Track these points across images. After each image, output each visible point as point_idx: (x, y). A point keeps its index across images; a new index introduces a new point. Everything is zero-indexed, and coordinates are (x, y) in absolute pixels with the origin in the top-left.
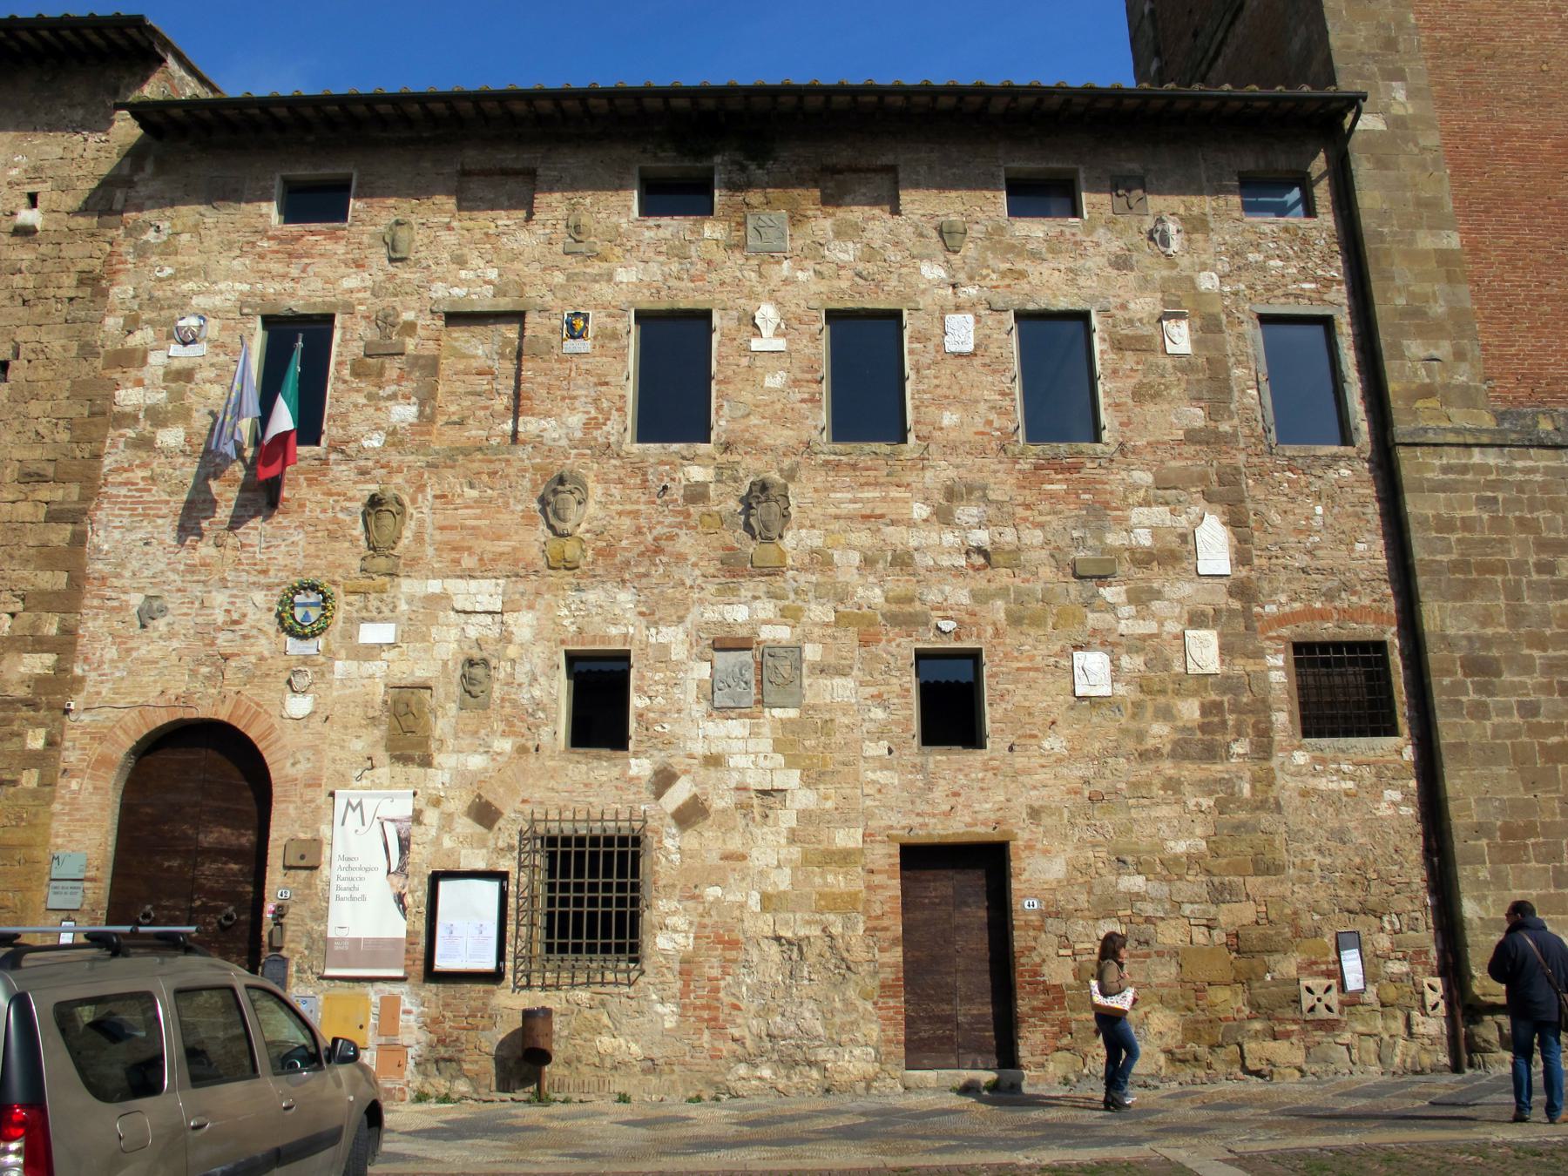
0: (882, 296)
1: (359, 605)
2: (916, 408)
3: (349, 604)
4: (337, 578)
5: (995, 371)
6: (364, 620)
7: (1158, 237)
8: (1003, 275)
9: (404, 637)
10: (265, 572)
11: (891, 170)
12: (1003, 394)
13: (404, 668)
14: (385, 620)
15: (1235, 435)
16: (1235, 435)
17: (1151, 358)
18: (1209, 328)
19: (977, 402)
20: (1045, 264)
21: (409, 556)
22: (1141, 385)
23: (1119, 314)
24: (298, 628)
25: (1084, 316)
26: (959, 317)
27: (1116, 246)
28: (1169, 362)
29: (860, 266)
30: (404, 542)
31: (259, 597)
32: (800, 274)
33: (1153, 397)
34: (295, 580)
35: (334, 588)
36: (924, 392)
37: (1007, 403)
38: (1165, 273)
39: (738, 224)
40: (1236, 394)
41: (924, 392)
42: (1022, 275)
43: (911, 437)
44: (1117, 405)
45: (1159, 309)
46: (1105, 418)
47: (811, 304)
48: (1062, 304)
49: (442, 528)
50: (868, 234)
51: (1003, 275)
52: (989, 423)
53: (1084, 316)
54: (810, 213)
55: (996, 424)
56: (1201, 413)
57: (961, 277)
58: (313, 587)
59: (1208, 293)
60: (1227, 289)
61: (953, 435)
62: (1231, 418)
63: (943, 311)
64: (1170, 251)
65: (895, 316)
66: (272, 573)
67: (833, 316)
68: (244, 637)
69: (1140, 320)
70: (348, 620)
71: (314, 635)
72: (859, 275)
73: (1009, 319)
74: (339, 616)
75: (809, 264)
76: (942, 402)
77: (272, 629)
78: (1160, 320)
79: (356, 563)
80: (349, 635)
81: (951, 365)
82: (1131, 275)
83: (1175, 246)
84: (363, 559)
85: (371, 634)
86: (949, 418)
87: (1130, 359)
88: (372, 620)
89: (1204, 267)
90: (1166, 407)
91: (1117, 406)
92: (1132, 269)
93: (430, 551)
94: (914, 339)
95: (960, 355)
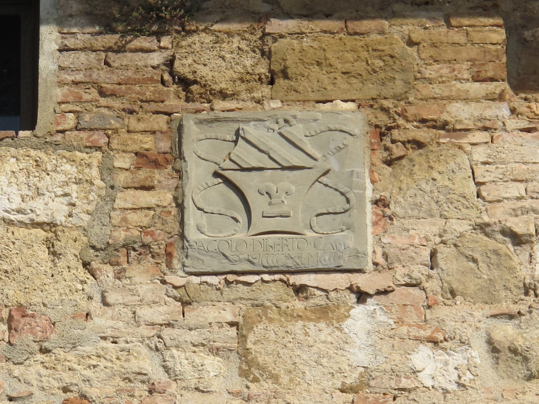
32: (423, 358)
39: (144, 158)
54: (460, 113)
75: (468, 318)
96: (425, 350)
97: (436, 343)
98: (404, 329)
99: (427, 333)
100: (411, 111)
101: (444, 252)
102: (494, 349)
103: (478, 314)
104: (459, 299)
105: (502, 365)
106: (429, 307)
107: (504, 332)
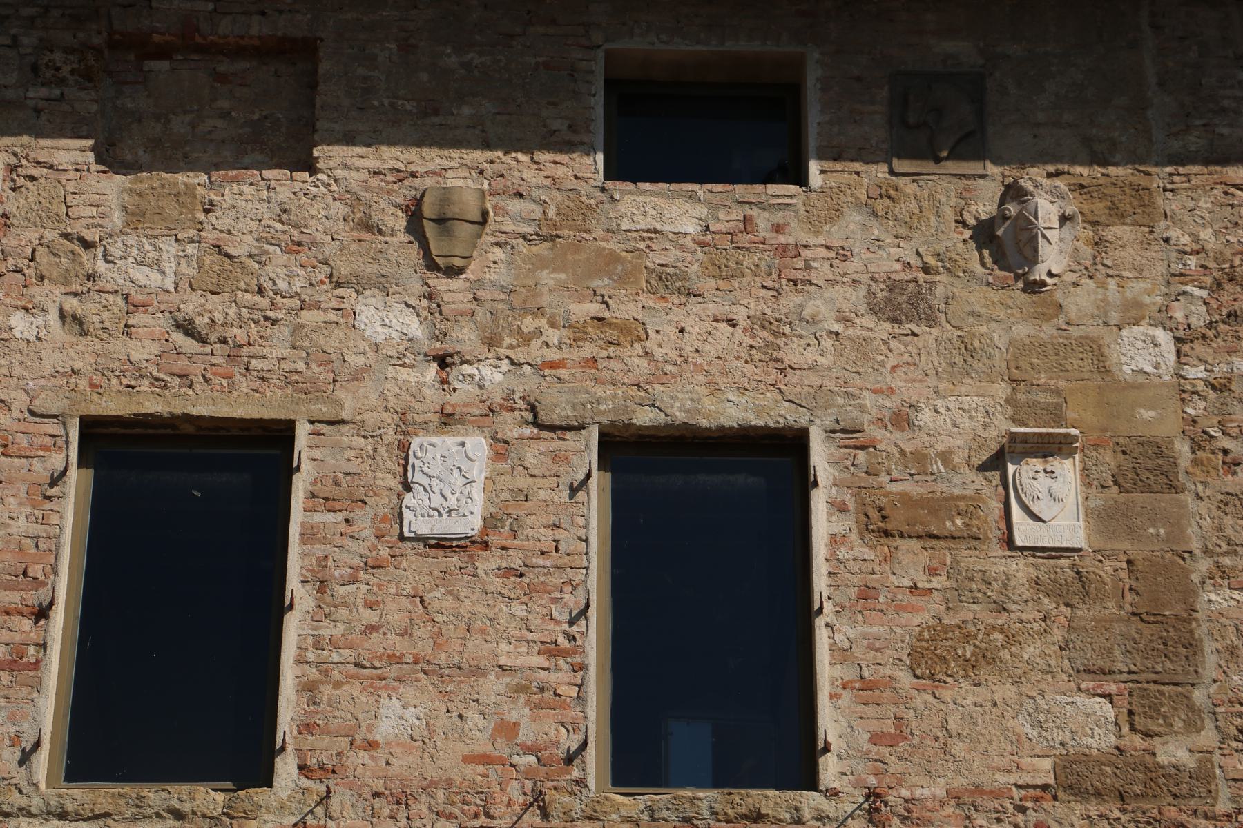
0: (244, 385)
2: (308, 688)
5: (532, 591)
7: (1005, 244)
8: (578, 333)
11: (300, 51)
12: (551, 651)
15: (1203, 775)
16: (1203, 775)
17: (970, 559)
18: (1139, 476)
19: (479, 671)
20: (694, 306)
22: (938, 631)
23: (887, 439)
25: (788, 447)
26: (448, 442)
27: (891, 259)
28: (1020, 569)
29: (191, 305)
33: (970, 665)
36: (335, 644)
37: (561, 678)
38: (1022, 331)
40: (1210, 662)
41: (335, 644)
42: (633, 332)
43: (286, 769)
44: (869, 686)
45: (1003, 426)
46: (830, 721)
47: (45, 403)
48: (732, 410)
50: (221, 219)
51: (578, 333)
52: (508, 730)
53: (788, 447)
55: (526, 735)
56: (1105, 709)
57: (466, 337)
59: (1142, 384)
60: (1196, 373)
61: (404, 763)
62: (1192, 726)
63: (406, 426)
64: (1040, 273)
65: (269, 445)
67: (102, 439)
69: (945, 457)
72: (187, 328)
73: (584, 450)
75: (52, 296)
76: (379, 673)
78: (996, 462)
81: (417, 570)
82: (929, 335)
83: (1054, 256)
86: (395, 716)
87: (912, 560)
89: (1133, 314)
90: (1005, 691)
91: (866, 688)
92: (931, 321)
94: (320, 500)
95: (441, 544)
96: (20, 314)
97: (27, 310)
98: (8, 300)
99: (23, 303)
100: (32, 155)
101: (41, 250)
102: (62, 315)
103: (57, 292)
104: (46, 281)
105: (67, 325)
106: (25, 286)
107: (72, 304)
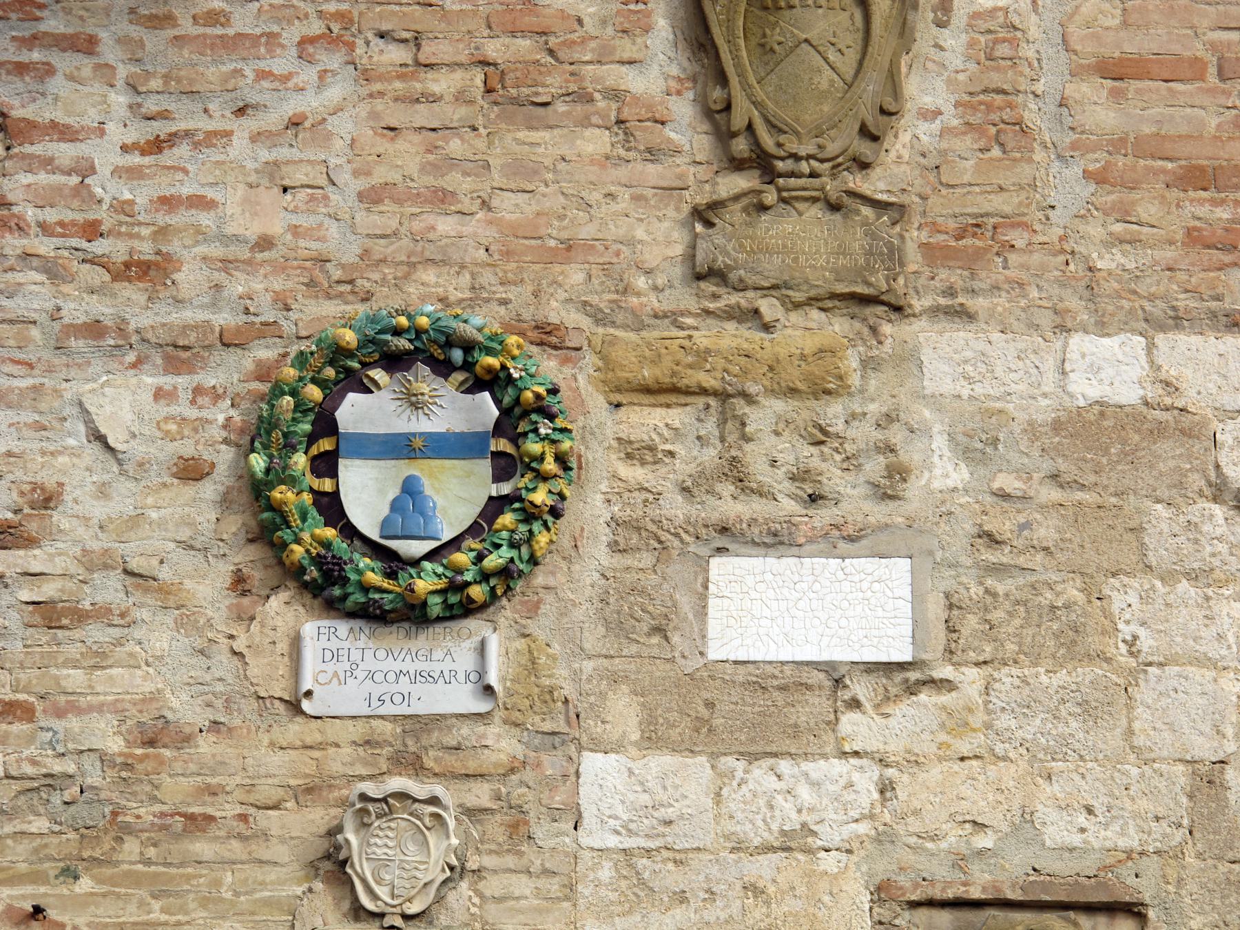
1: (692, 457)
3: (636, 452)
4: (556, 311)
6: (727, 536)
9: (953, 624)
10: (149, 271)
13: (979, 802)
14: (847, 539)
21: (943, 208)
24: (370, 571)
30: (910, 138)
31: (124, 401)
34: (340, 321)
35: (549, 367)
49: (1116, 71)
58: (443, 353)
66: (189, 277)
68: (49, 615)
70: (634, 532)
71: (460, 606)
74: (591, 508)
77: (208, 588)
79: (661, 239)
80: (652, 623)
84: (705, 215)
85: (776, 609)
88: (777, 540)
93: (1066, 187)
